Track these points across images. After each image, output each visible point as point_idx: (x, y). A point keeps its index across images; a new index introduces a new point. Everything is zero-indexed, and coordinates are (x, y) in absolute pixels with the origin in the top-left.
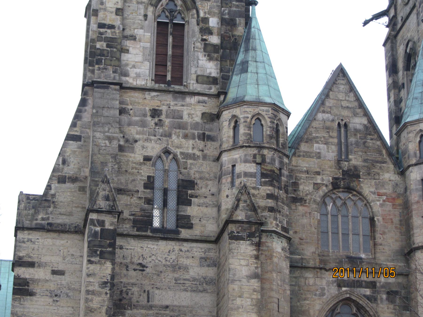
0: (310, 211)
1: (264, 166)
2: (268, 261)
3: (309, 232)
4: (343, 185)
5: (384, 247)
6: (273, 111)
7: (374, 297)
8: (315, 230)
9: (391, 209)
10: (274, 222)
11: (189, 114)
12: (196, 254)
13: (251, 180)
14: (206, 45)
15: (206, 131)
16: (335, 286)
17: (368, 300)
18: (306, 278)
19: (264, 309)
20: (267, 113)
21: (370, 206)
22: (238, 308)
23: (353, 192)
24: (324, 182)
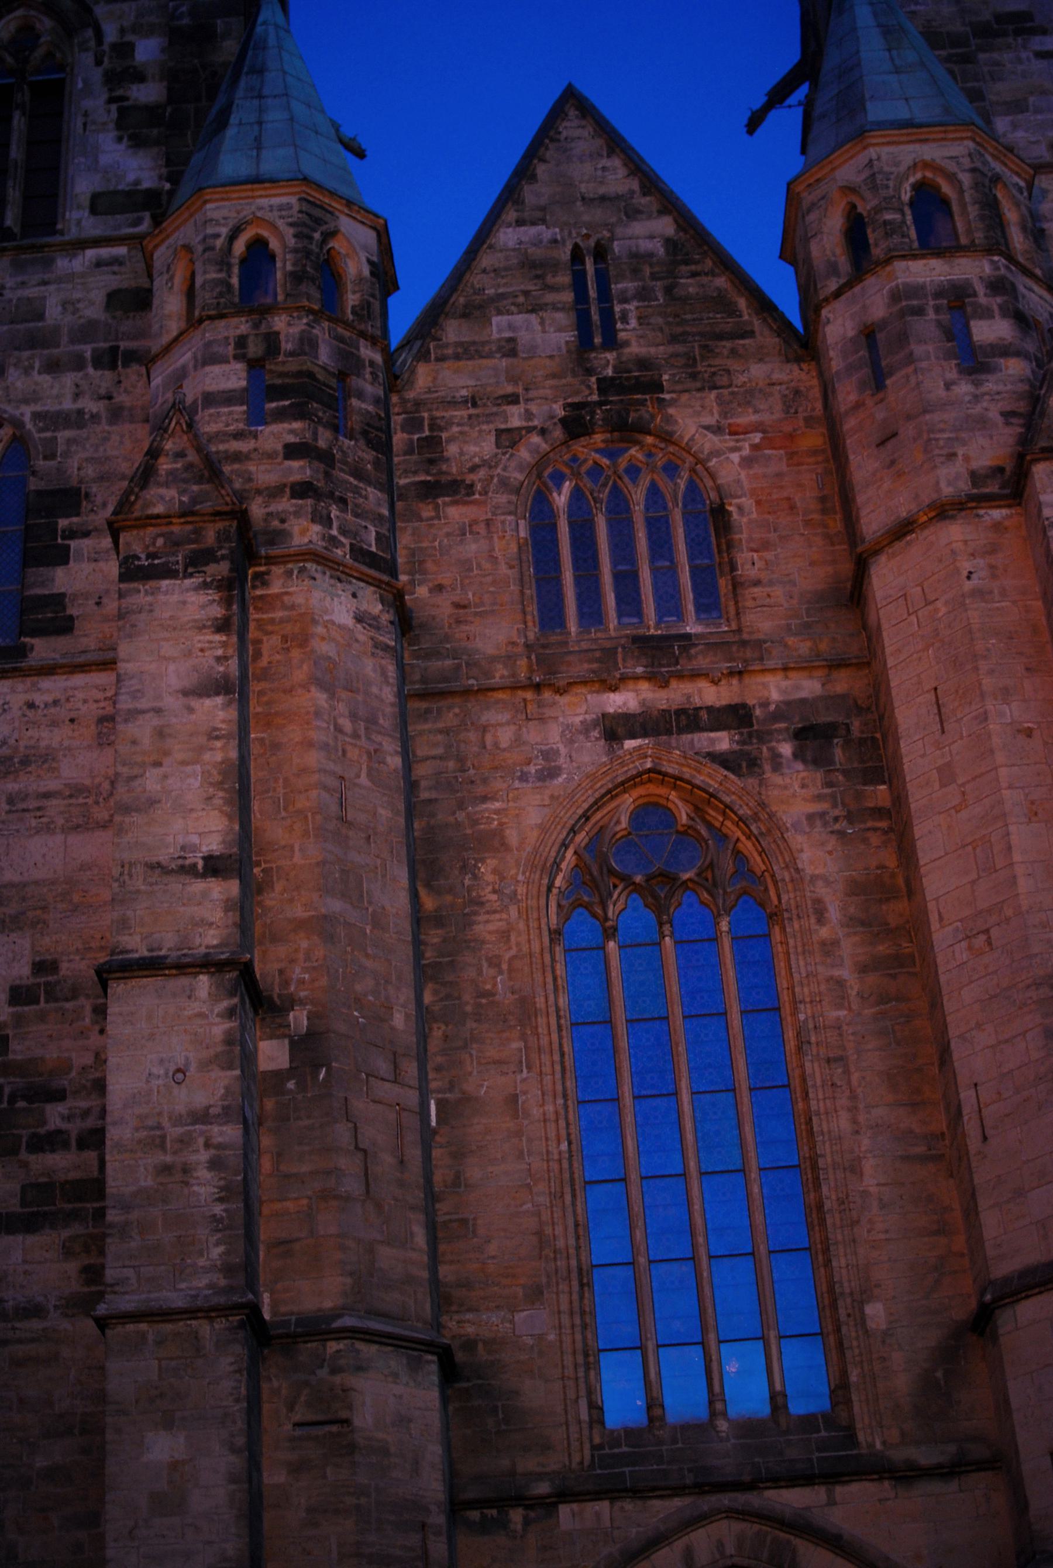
0: (489, 516)
1: (276, 364)
2: (296, 653)
3: (489, 579)
4: (603, 420)
5: (768, 589)
6: (304, 204)
7: (748, 753)
8: (509, 572)
9: (784, 468)
10: (316, 528)
11: (65, 304)
12: (84, 708)
13: (230, 413)
14: (121, 111)
15: (122, 339)
16: (597, 739)
17: (727, 768)
18: (485, 729)
19: (283, 814)
20: (284, 213)
21: (707, 469)
22: (153, 802)
23: (640, 437)
24: (536, 423)
